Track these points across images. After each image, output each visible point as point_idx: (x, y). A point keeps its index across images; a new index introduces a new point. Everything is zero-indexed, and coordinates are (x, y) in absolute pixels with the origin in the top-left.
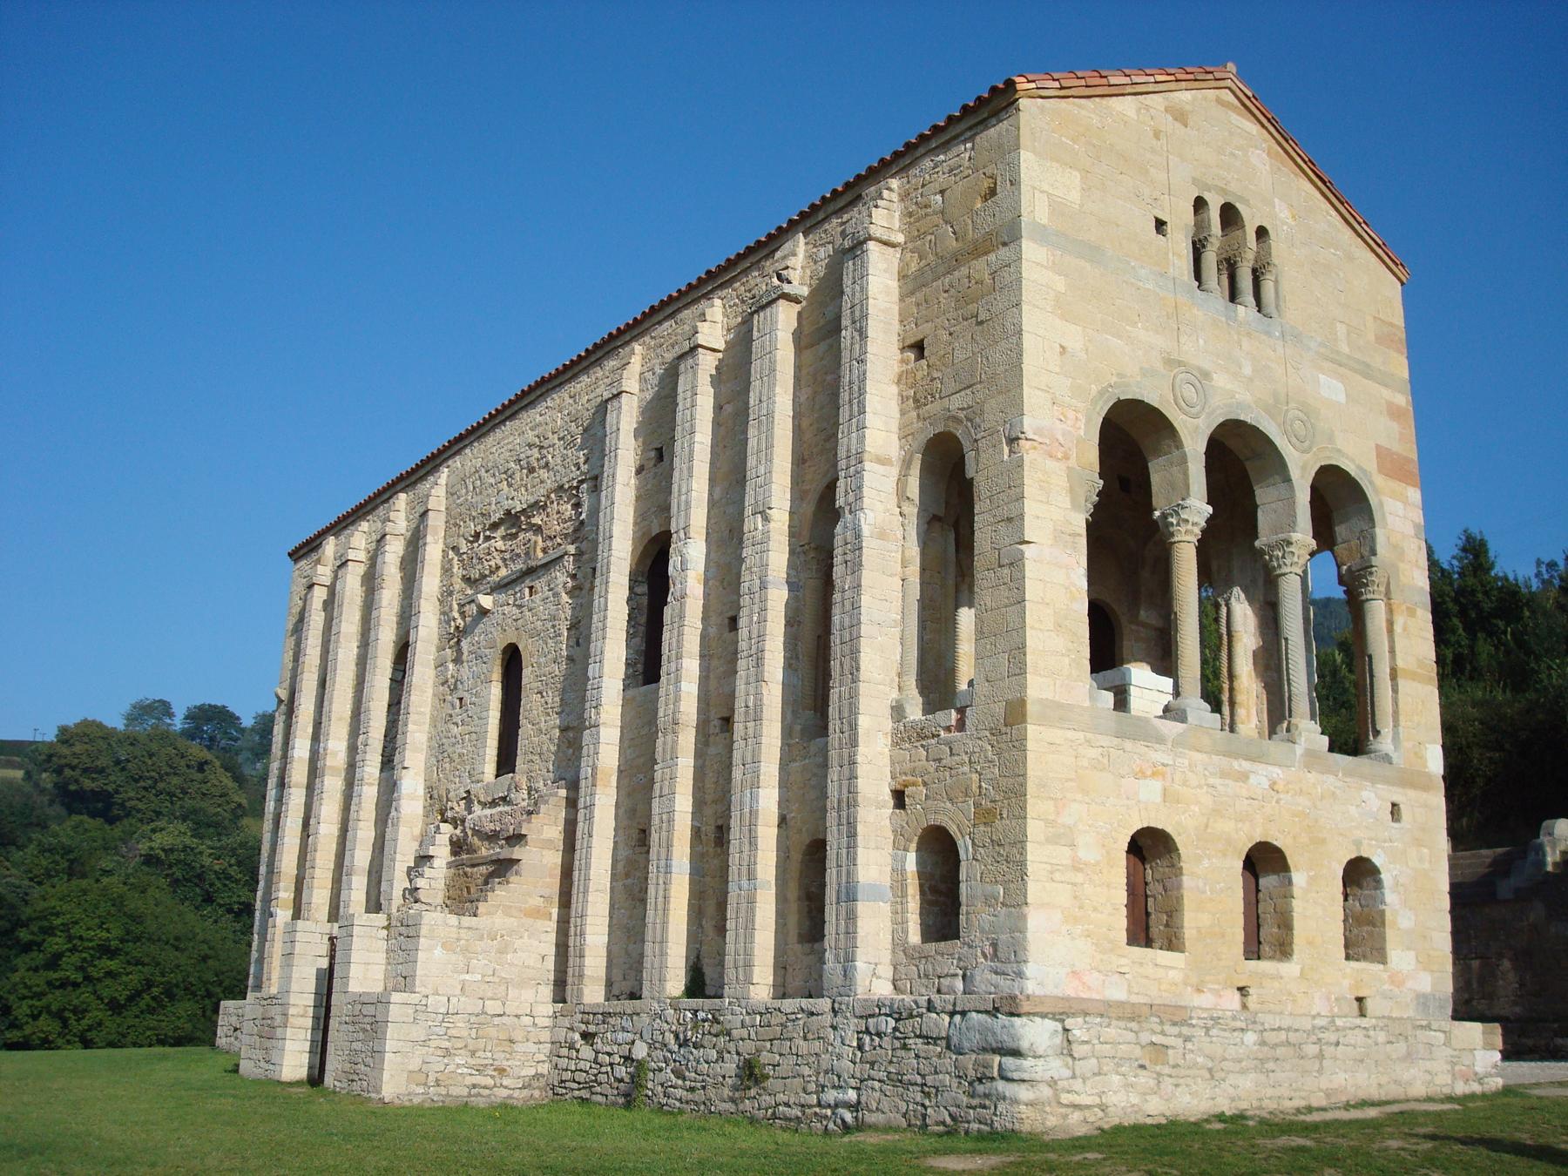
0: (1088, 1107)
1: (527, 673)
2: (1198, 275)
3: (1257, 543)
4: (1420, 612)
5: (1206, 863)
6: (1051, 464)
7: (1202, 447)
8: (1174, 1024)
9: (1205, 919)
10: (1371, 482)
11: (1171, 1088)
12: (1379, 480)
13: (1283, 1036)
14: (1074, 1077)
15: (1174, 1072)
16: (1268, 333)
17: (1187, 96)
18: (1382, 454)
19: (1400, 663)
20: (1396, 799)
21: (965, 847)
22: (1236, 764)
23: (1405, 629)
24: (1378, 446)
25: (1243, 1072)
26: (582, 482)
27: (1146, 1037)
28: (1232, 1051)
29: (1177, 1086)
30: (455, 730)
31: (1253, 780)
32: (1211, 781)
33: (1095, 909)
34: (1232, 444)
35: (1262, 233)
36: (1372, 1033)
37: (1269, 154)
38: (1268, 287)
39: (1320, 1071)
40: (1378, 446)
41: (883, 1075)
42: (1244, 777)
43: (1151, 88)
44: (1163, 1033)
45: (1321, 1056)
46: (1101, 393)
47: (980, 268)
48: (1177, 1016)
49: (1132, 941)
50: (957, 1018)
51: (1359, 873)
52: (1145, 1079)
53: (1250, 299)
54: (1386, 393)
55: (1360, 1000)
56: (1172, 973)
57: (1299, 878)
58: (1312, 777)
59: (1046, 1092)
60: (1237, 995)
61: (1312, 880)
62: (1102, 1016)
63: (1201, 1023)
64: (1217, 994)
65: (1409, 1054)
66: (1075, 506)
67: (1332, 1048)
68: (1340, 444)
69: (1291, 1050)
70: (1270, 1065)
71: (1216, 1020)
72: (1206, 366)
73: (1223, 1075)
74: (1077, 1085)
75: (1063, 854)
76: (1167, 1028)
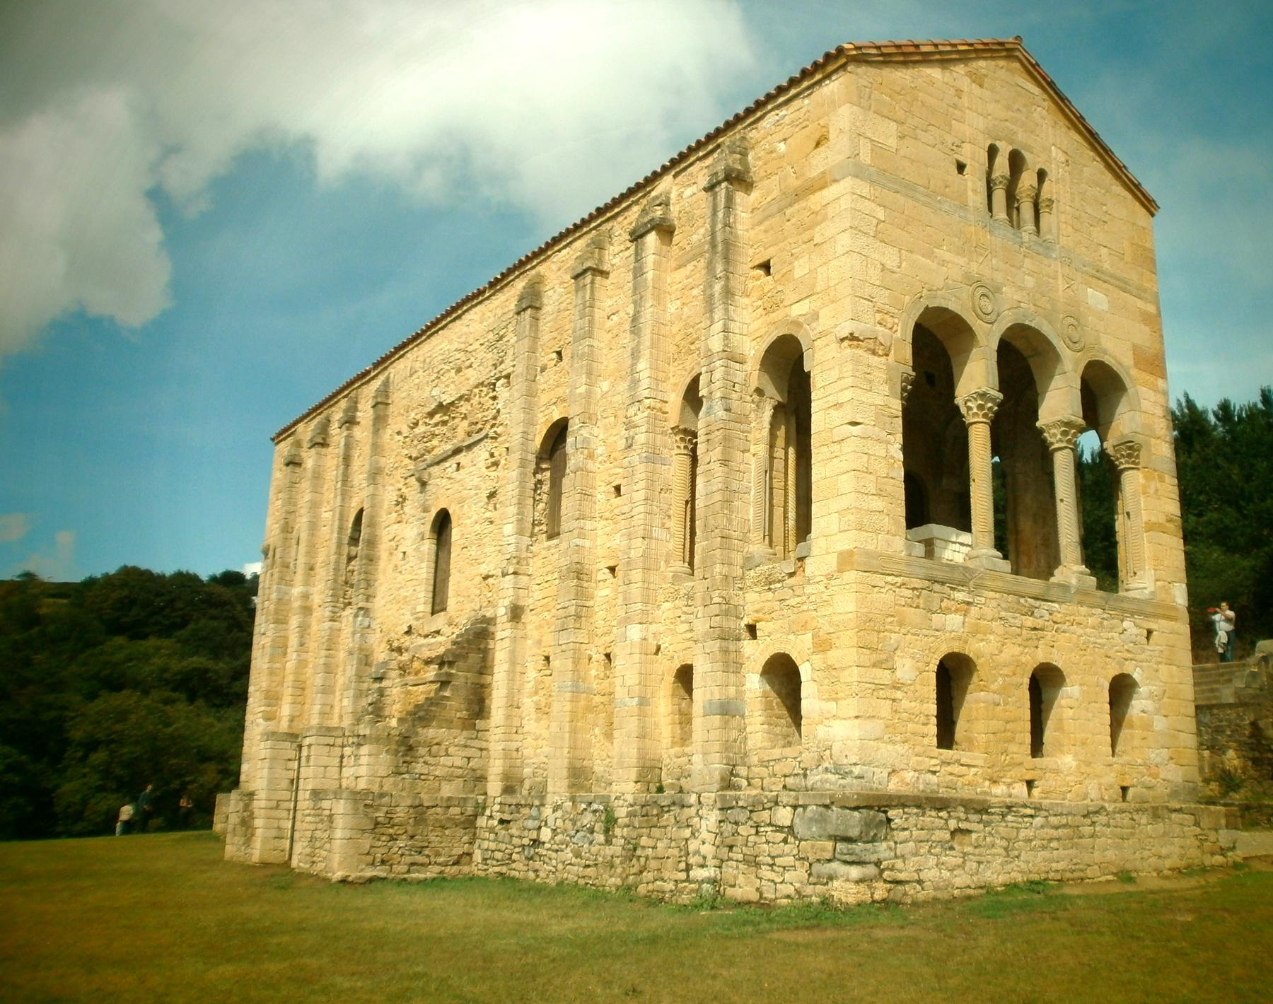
0: (908, 882)
1: (455, 533)
2: (990, 209)
3: (1038, 424)
5: (1000, 680)
6: (875, 360)
10: (1128, 374)
11: (975, 865)
12: (1134, 372)
13: (1064, 821)
14: (896, 857)
15: (977, 851)
16: (1048, 257)
17: (982, 63)
18: (1136, 350)
20: (1152, 626)
21: (805, 672)
22: (1022, 600)
24: (1134, 345)
26: (498, 379)
27: (953, 824)
28: (1022, 834)
29: (979, 863)
30: (400, 577)
32: (1003, 614)
33: (910, 720)
34: (1019, 344)
35: (1042, 175)
36: (1136, 817)
38: (1044, 218)
40: (1134, 345)
41: (740, 857)
43: (954, 56)
44: (967, 820)
47: (816, 200)
48: (981, 808)
49: (940, 745)
50: (800, 809)
51: (1121, 690)
52: (952, 859)
53: (1030, 227)
54: (1140, 303)
55: (1124, 789)
56: (973, 770)
58: (1084, 609)
59: (871, 870)
62: (918, 807)
63: (997, 810)
65: (1164, 834)
66: (892, 395)
71: (1009, 807)
73: (1016, 853)
74: (899, 863)
75: (884, 676)
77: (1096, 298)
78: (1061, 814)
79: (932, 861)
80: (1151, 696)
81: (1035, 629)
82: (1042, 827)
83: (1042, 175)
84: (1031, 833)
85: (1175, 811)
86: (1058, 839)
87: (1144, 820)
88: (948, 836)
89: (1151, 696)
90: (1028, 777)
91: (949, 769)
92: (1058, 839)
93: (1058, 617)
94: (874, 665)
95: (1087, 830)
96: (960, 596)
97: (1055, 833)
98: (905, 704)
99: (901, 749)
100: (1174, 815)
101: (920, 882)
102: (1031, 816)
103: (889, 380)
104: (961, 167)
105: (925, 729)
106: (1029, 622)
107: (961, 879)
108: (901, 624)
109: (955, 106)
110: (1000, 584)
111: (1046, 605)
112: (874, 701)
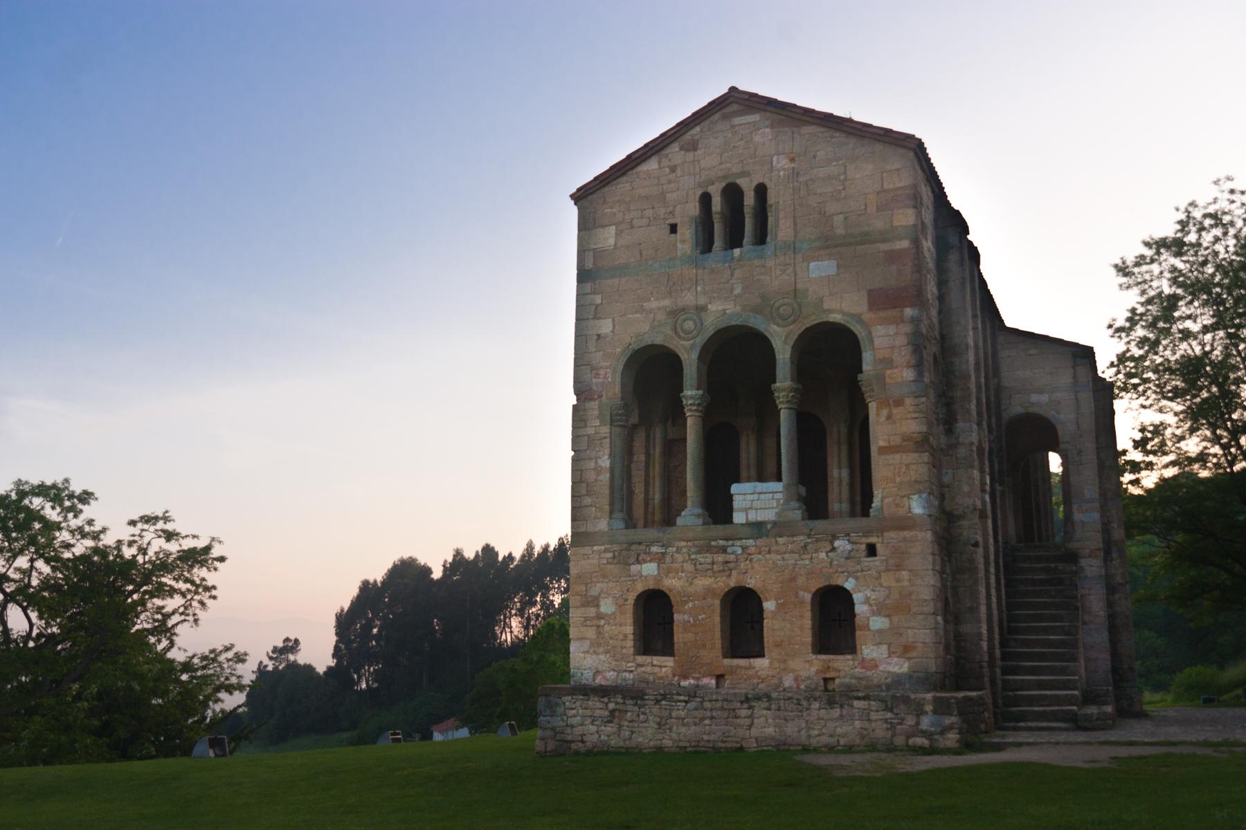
4: (908, 401)
5: (690, 605)
7: (695, 356)
8: (632, 698)
9: (690, 636)
16: (761, 257)
17: (698, 129)
19: (882, 443)
20: (873, 540)
22: (713, 543)
23: (889, 417)
25: (684, 725)
27: (611, 706)
29: (633, 732)
31: (729, 550)
37: (772, 127)
39: (750, 726)
42: (724, 550)
45: (751, 717)
46: (624, 351)
52: (610, 729)
57: (769, 605)
58: (780, 540)
60: (713, 682)
61: (779, 606)
64: (698, 679)
66: (602, 423)
67: (765, 712)
68: (826, 306)
69: (726, 714)
70: (707, 722)
71: (664, 697)
72: (702, 301)
74: (569, 730)
75: (592, 612)
76: (628, 702)
77: (821, 269)
78: (717, 700)
79: (593, 728)
80: (867, 601)
81: (727, 562)
82: (696, 709)
83: (761, 191)
84: (682, 714)
85: (858, 698)
86: (712, 718)
87: (816, 705)
88: (607, 713)
89: (867, 601)
90: (718, 673)
91: (643, 669)
92: (712, 718)
93: (752, 550)
94: (583, 606)
95: (744, 712)
96: (654, 549)
97: (708, 714)
98: (607, 628)
99: (602, 657)
100: (856, 703)
101: (582, 741)
102: (686, 702)
103: (601, 416)
104: (673, 229)
105: (624, 644)
106: (720, 558)
107: (613, 742)
108: (604, 576)
109: (670, 182)
110: (691, 535)
111: (738, 543)
112: (583, 629)
